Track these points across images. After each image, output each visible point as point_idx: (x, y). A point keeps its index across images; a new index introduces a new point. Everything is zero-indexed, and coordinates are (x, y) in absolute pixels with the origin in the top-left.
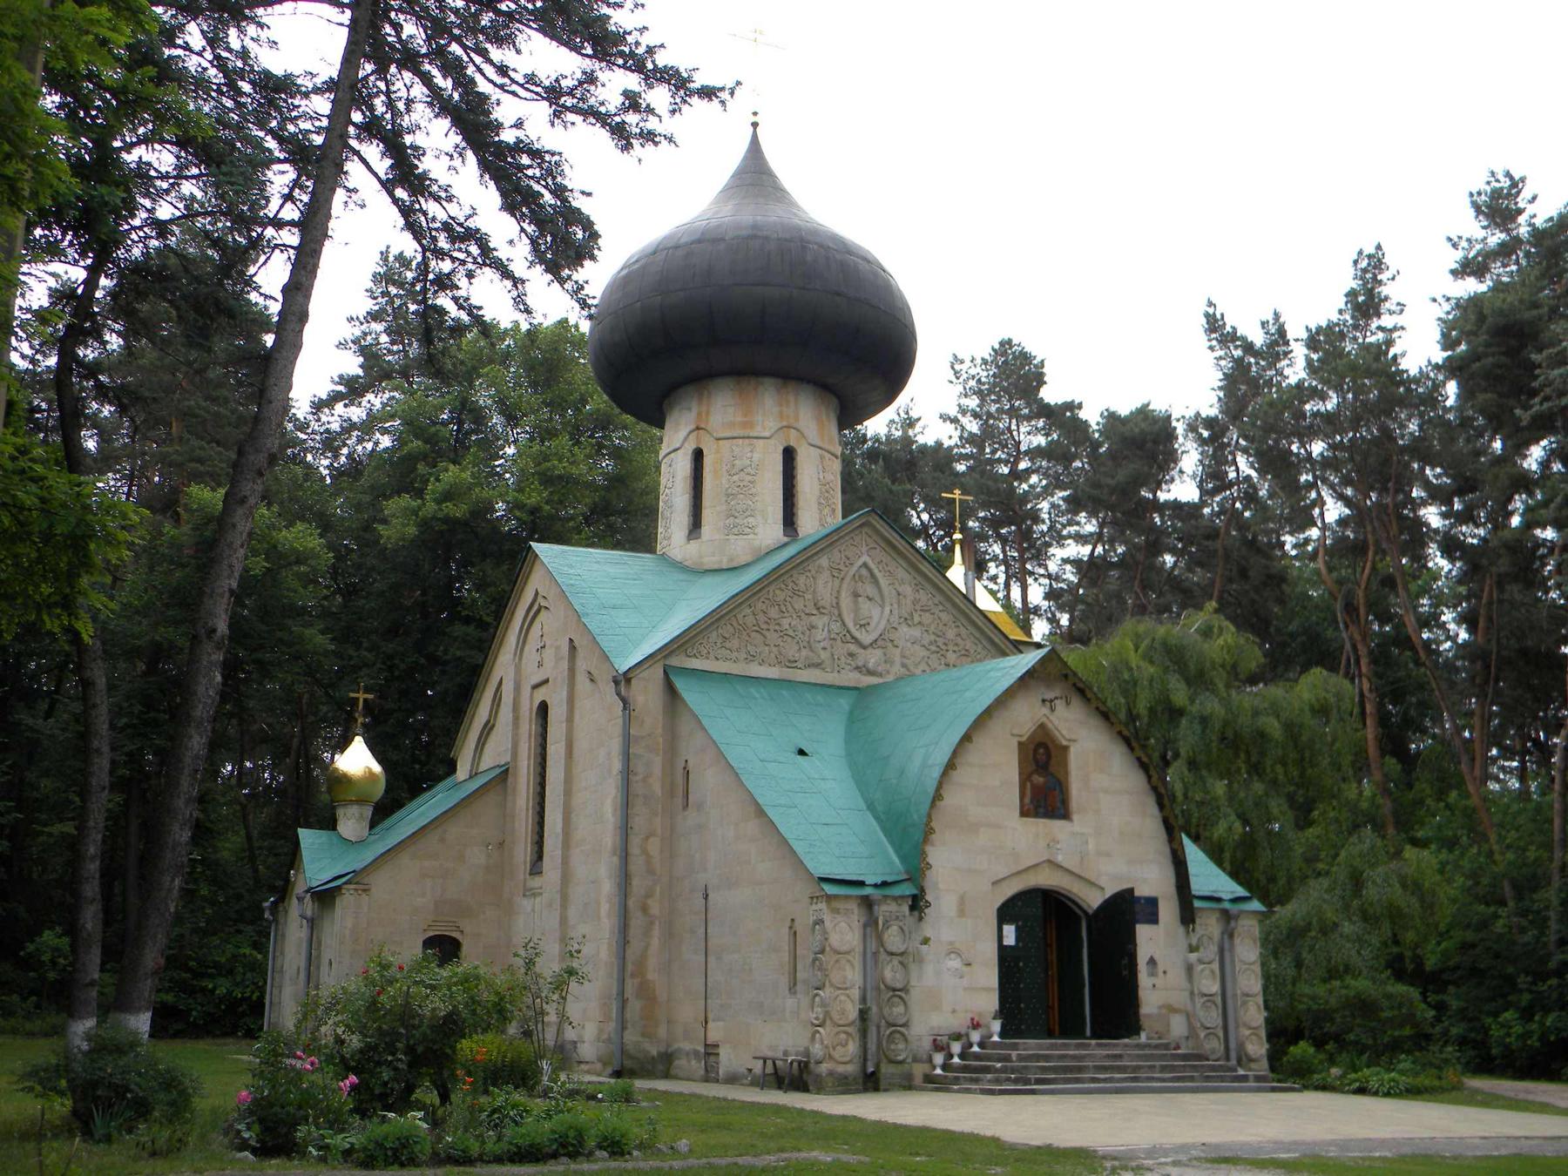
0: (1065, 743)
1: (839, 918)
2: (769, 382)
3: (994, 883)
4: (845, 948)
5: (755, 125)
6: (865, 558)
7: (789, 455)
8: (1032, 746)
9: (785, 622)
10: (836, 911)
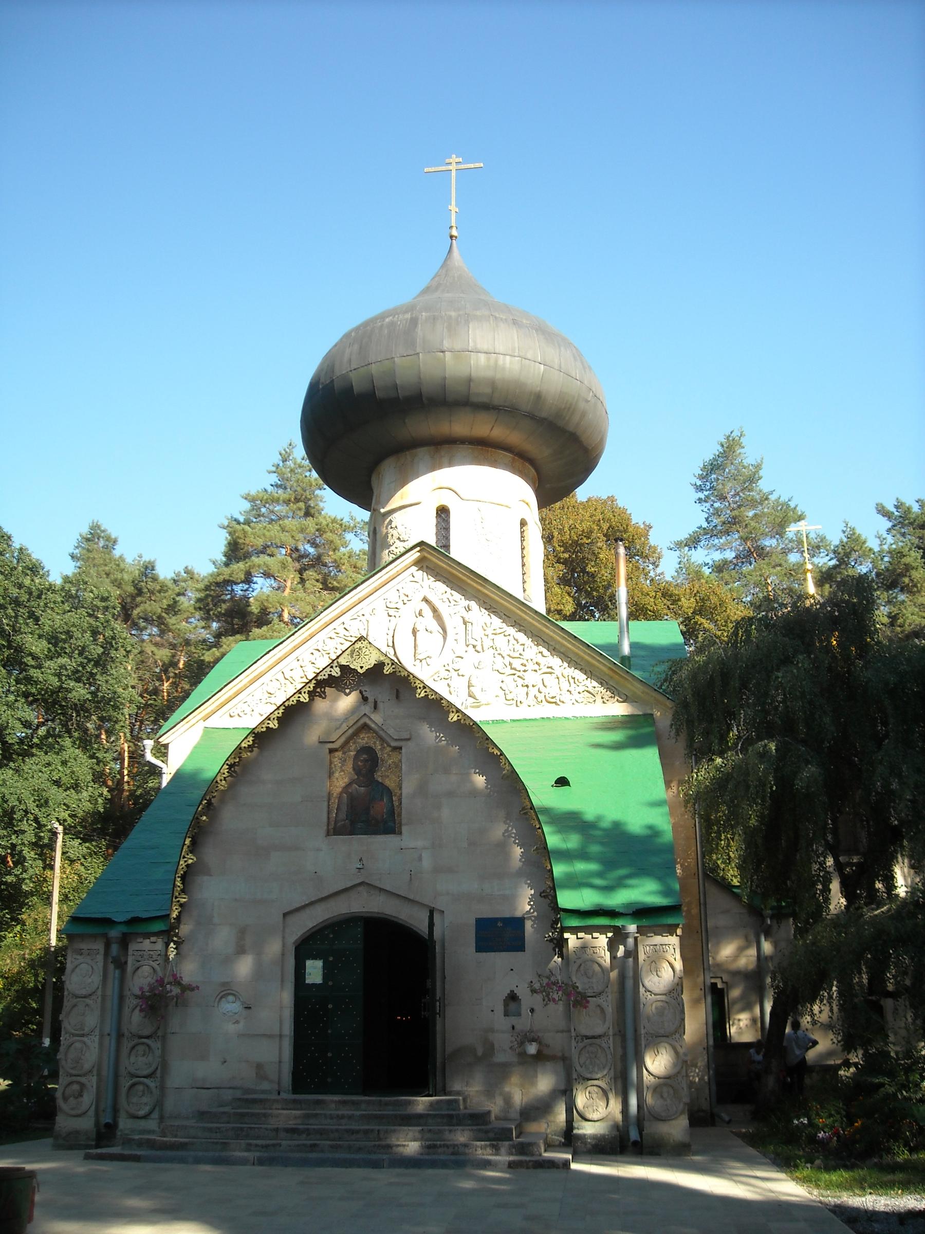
0: (394, 744)
1: (81, 959)
3: (285, 915)
4: (84, 992)
7: (443, 513)
8: (352, 753)
10: (80, 952)
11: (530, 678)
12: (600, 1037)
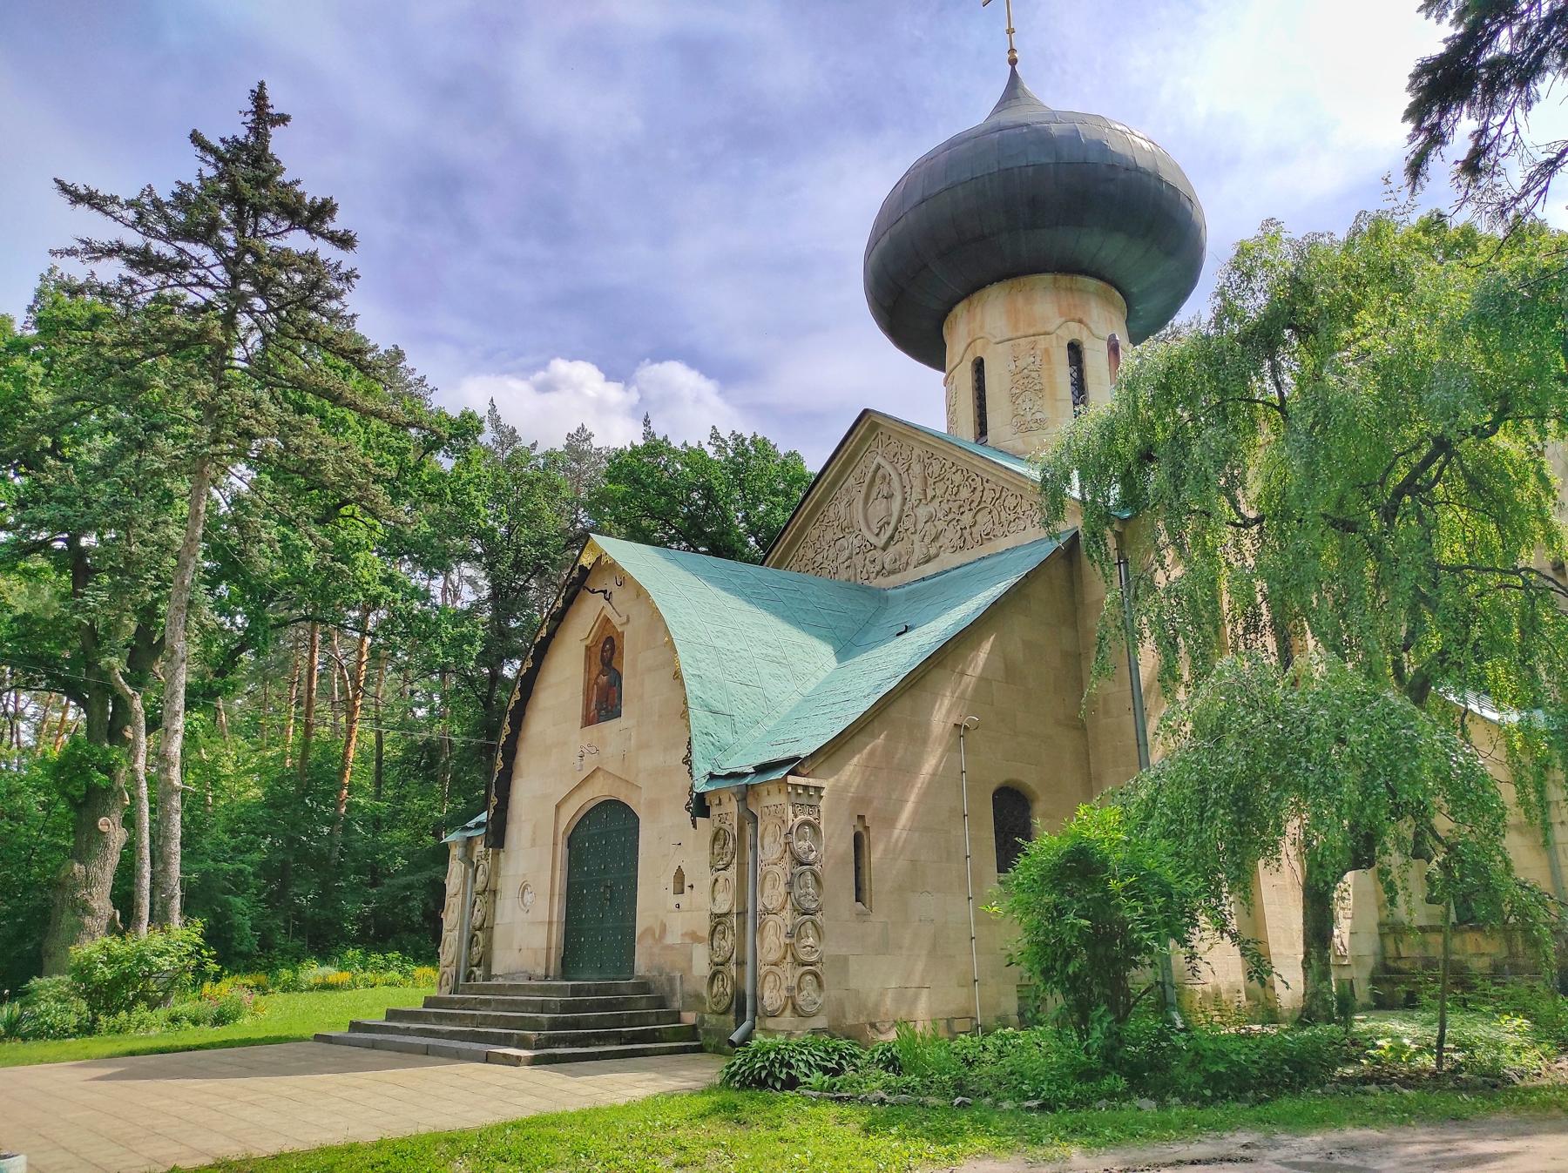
2: (960, 309)
3: (558, 807)
5: (1013, 62)
6: (879, 459)
9: (819, 559)
11: (967, 519)
12: (725, 915)
